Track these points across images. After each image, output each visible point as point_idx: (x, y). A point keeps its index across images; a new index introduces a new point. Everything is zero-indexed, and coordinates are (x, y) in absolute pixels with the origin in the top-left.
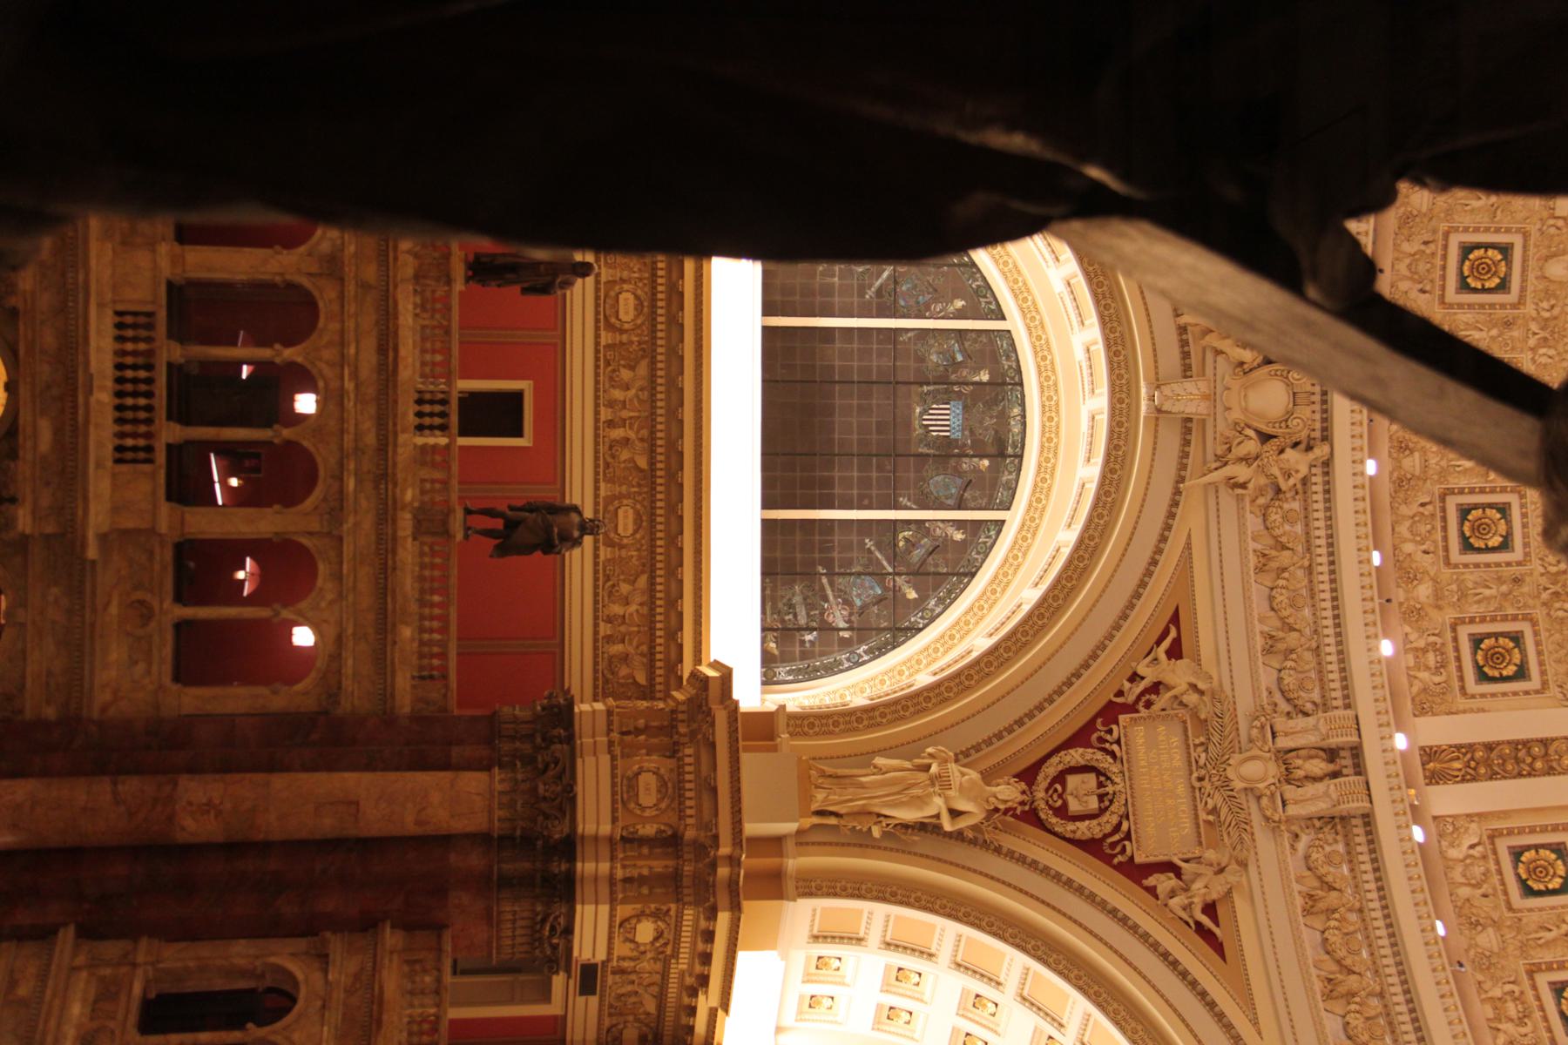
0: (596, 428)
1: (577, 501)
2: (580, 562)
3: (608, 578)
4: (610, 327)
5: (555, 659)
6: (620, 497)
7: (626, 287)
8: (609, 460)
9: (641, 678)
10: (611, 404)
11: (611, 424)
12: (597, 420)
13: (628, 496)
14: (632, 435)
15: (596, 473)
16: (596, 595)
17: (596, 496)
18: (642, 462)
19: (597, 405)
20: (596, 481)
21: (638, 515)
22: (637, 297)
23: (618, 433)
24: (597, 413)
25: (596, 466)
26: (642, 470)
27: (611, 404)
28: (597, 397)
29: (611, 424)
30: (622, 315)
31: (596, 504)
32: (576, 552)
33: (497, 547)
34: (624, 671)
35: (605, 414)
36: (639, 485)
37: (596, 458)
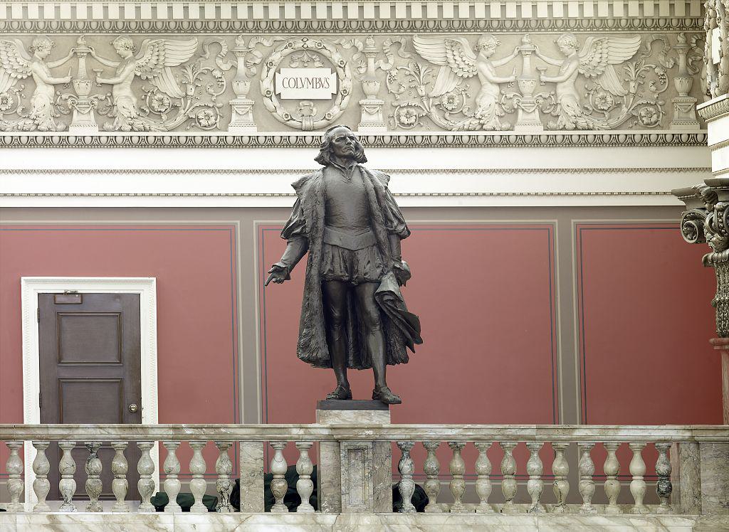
0: (112, 144)
1: (285, 184)
2: (416, 179)
3: (425, 118)
4: (226, 112)
5: (604, 230)
6: (257, 94)
7: (266, 85)
8: (180, 119)
9: (627, 46)
10: (64, 113)
11: (106, 111)
12: (95, 143)
13: (255, 79)
14: (129, 70)
15: (206, 144)
16: (458, 143)
17: (254, 143)
18: (180, 50)
19: (64, 143)
20: (222, 144)
21: (294, 57)
22: (291, 58)
23: (125, 100)
24: (81, 143)
25: (190, 144)
26: (200, 54)
27: (64, 113)
28: (48, 143)
29: (106, 111)
30: (326, 94)
31: (285, 144)
32: (396, 186)
33: (418, 343)
34: (612, 83)
35: (85, 126)
36: (233, 54)
37: (175, 144)
